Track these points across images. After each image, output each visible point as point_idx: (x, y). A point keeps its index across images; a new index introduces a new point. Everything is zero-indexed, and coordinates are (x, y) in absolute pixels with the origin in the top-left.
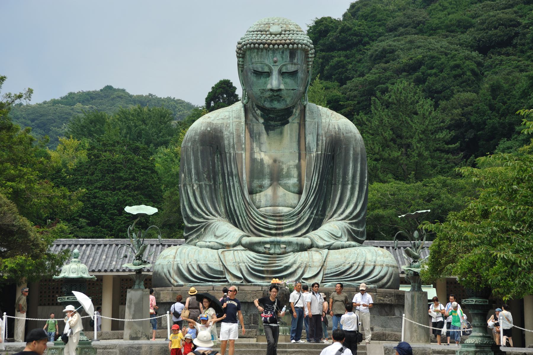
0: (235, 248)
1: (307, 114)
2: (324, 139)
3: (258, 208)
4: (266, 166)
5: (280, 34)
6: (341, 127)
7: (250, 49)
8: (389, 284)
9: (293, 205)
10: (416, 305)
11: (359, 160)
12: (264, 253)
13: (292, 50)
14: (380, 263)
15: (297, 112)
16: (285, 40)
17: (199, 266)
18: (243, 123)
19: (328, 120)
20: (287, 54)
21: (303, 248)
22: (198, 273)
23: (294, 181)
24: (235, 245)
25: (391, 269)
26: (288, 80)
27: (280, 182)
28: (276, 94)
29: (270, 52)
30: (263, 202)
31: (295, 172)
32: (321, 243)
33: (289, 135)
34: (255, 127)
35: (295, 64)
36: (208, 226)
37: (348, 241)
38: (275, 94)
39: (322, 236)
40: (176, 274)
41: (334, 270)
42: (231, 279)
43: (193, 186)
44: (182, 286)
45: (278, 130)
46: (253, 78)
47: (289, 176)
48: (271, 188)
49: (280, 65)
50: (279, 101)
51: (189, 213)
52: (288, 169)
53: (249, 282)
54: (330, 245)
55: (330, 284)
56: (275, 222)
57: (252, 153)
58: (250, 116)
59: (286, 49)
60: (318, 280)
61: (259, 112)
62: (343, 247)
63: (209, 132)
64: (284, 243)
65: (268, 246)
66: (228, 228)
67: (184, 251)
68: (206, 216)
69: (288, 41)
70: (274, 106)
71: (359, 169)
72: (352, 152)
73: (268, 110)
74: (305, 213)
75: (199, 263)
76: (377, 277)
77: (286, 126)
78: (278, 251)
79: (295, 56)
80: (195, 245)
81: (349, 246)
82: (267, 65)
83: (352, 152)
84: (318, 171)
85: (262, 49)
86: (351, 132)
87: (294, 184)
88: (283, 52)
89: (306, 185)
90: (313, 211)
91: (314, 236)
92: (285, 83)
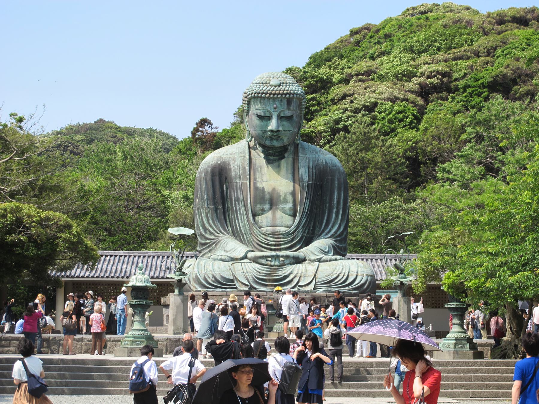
0: (242, 261)
1: (300, 151)
2: (314, 171)
3: (260, 228)
4: (266, 193)
5: (279, 86)
6: (328, 161)
7: (254, 97)
8: (368, 290)
9: (289, 226)
10: (401, 308)
11: (343, 189)
12: (266, 265)
13: (289, 99)
14: (362, 273)
15: (291, 148)
16: (284, 91)
17: (213, 276)
18: (248, 158)
19: (317, 156)
20: (285, 102)
21: (298, 261)
22: (213, 281)
23: (290, 205)
24: (242, 259)
26: (285, 123)
27: (278, 206)
28: (275, 134)
29: (271, 100)
30: (264, 224)
31: (290, 199)
32: (313, 257)
33: (285, 168)
34: (257, 161)
36: (219, 242)
37: (334, 255)
38: (275, 134)
39: (313, 251)
40: (195, 282)
41: (324, 279)
42: (240, 286)
43: (206, 209)
44: (200, 291)
45: (276, 164)
46: (256, 121)
47: (285, 201)
48: (271, 211)
50: (277, 140)
51: (203, 232)
52: (285, 196)
53: (255, 288)
54: (320, 259)
55: (321, 290)
56: (275, 240)
57: (255, 183)
58: (253, 152)
59: (284, 98)
60: (311, 287)
61: (260, 148)
62: (330, 260)
63: (219, 165)
64: (282, 256)
65: (270, 259)
66: (235, 244)
67: (201, 263)
68: (217, 235)
69: (285, 92)
70: (274, 144)
71: (342, 196)
72: (336, 182)
73: (268, 147)
74: (298, 232)
75: (213, 273)
76: (359, 284)
77: (283, 160)
78: (277, 263)
80: (209, 258)
81: (336, 260)
82: (268, 111)
83: (336, 182)
85: (264, 98)
86: (336, 166)
87: (290, 208)
88: (281, 100)
90: (305, 230)
91: (307, 251)
92: (283, 126)
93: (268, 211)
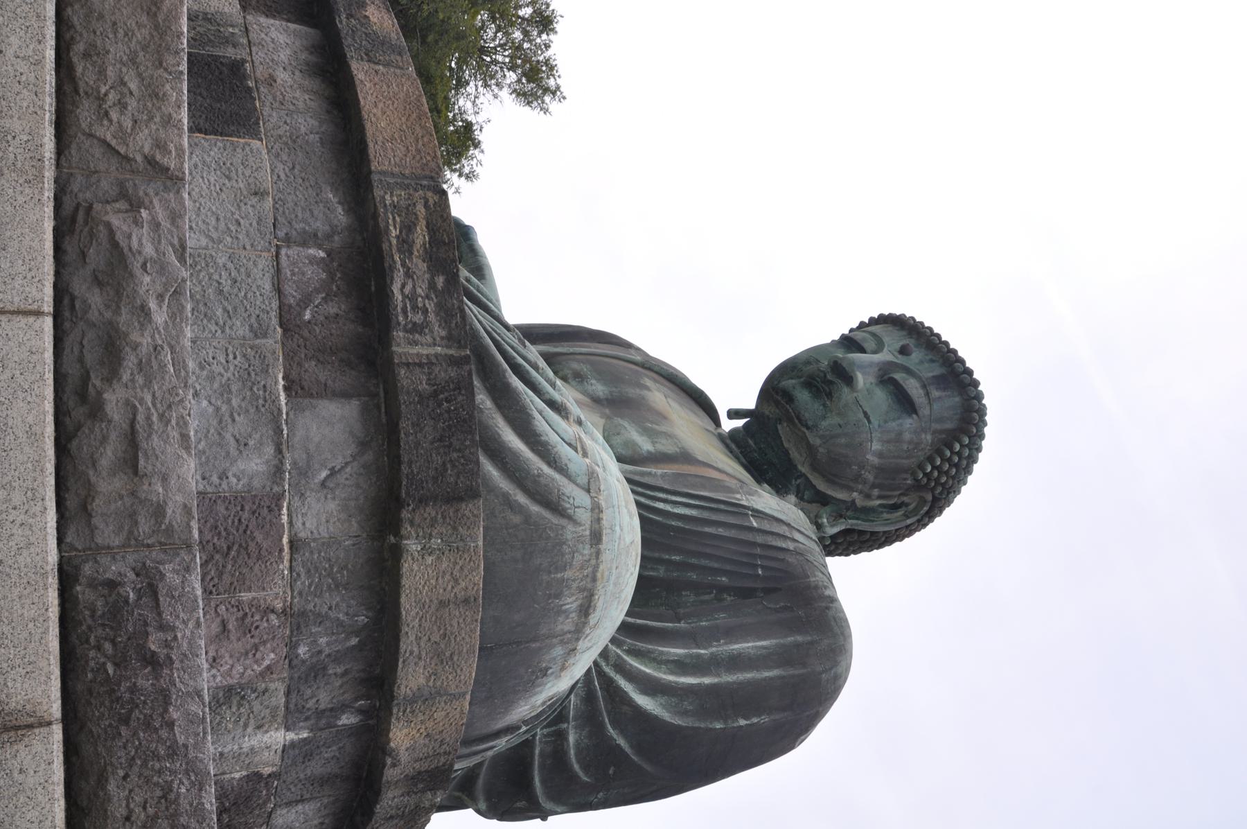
2: (791, 546)
20: (937, 370)
23: (646, 445)
25: (582, 498)
35: (927, 394)
49: (901, 360)
72: (800, 638)
79: (945, 389)
83: (800, 638)
84: (705, 515)
88: (932, 361)
89: (650, 474)
93: (585, 393)
